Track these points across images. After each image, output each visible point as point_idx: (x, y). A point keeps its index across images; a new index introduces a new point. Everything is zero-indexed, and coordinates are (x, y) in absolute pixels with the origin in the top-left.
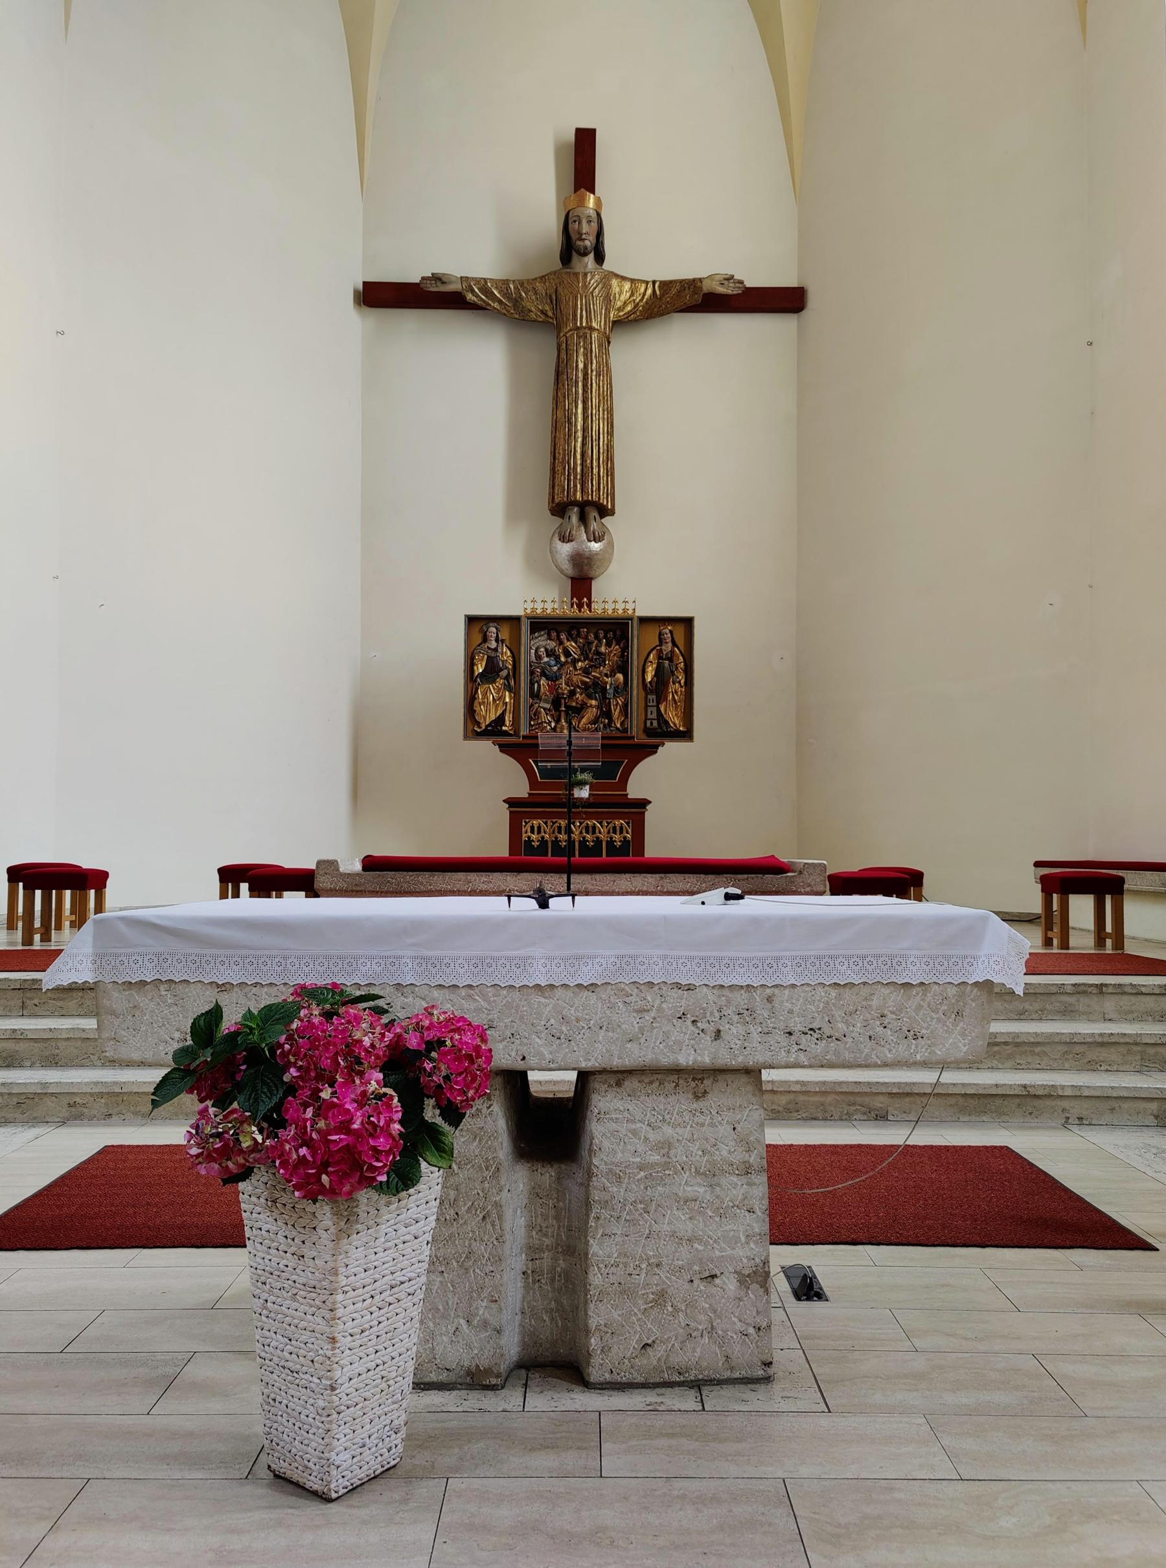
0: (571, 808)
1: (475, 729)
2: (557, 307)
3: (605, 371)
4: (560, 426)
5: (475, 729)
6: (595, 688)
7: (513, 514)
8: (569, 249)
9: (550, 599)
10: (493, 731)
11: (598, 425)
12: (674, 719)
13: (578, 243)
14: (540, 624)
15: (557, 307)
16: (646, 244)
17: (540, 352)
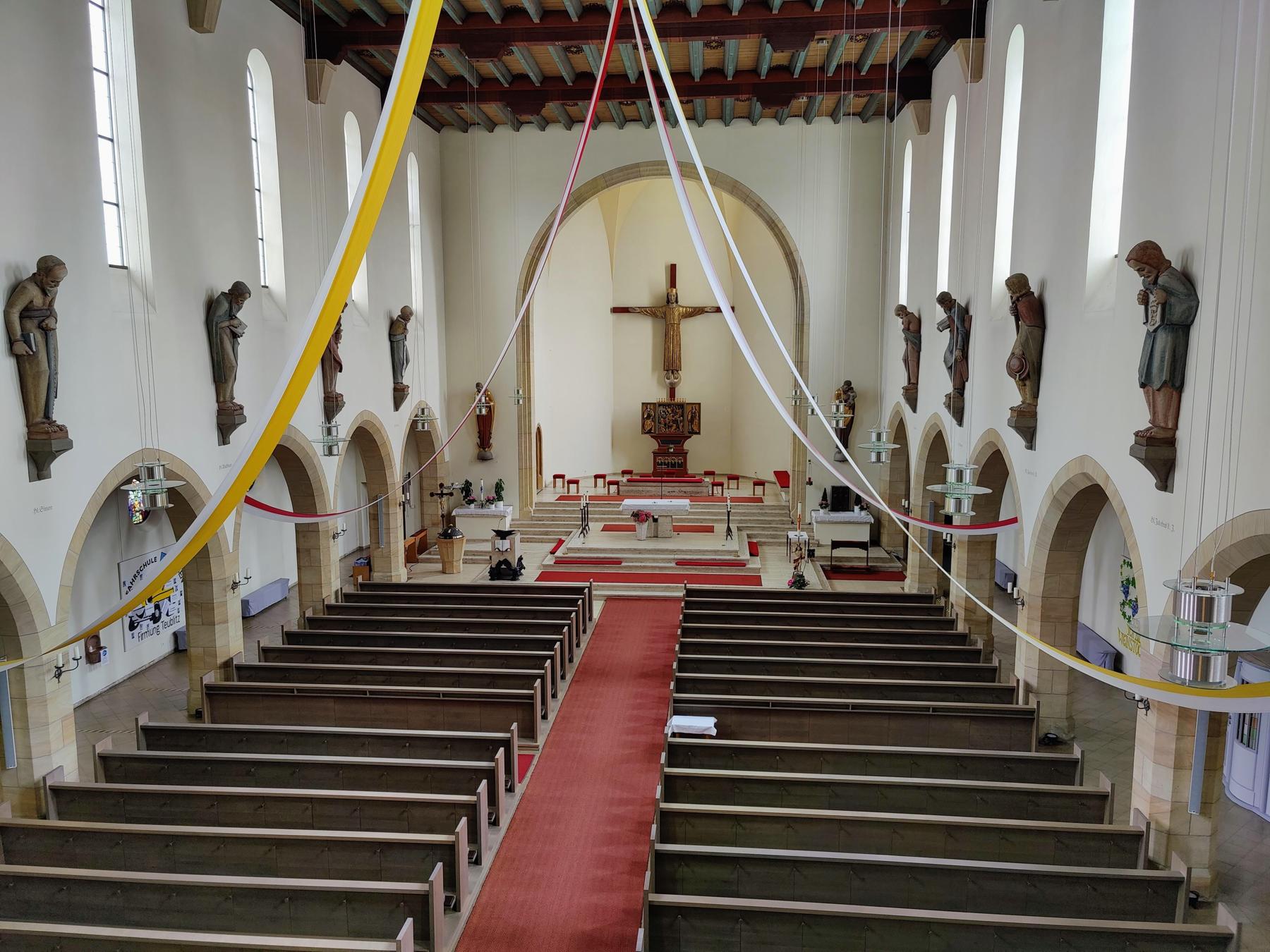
0: (668, 454)
1: (645, 431)
2: (666, 313)
3: (679, 334)
4: (666, 349)
5: (645, 431)
6: (675, 421)
7: (654, 369)
8: (668, 302)
9: (663, 396)
10: (649, 432)
11: (677, 350)
12: (696, 429)
13: (670, 300)
14: (660, 405)
15: (666, 313)
16: (688, 296)
17: (661, 325)
